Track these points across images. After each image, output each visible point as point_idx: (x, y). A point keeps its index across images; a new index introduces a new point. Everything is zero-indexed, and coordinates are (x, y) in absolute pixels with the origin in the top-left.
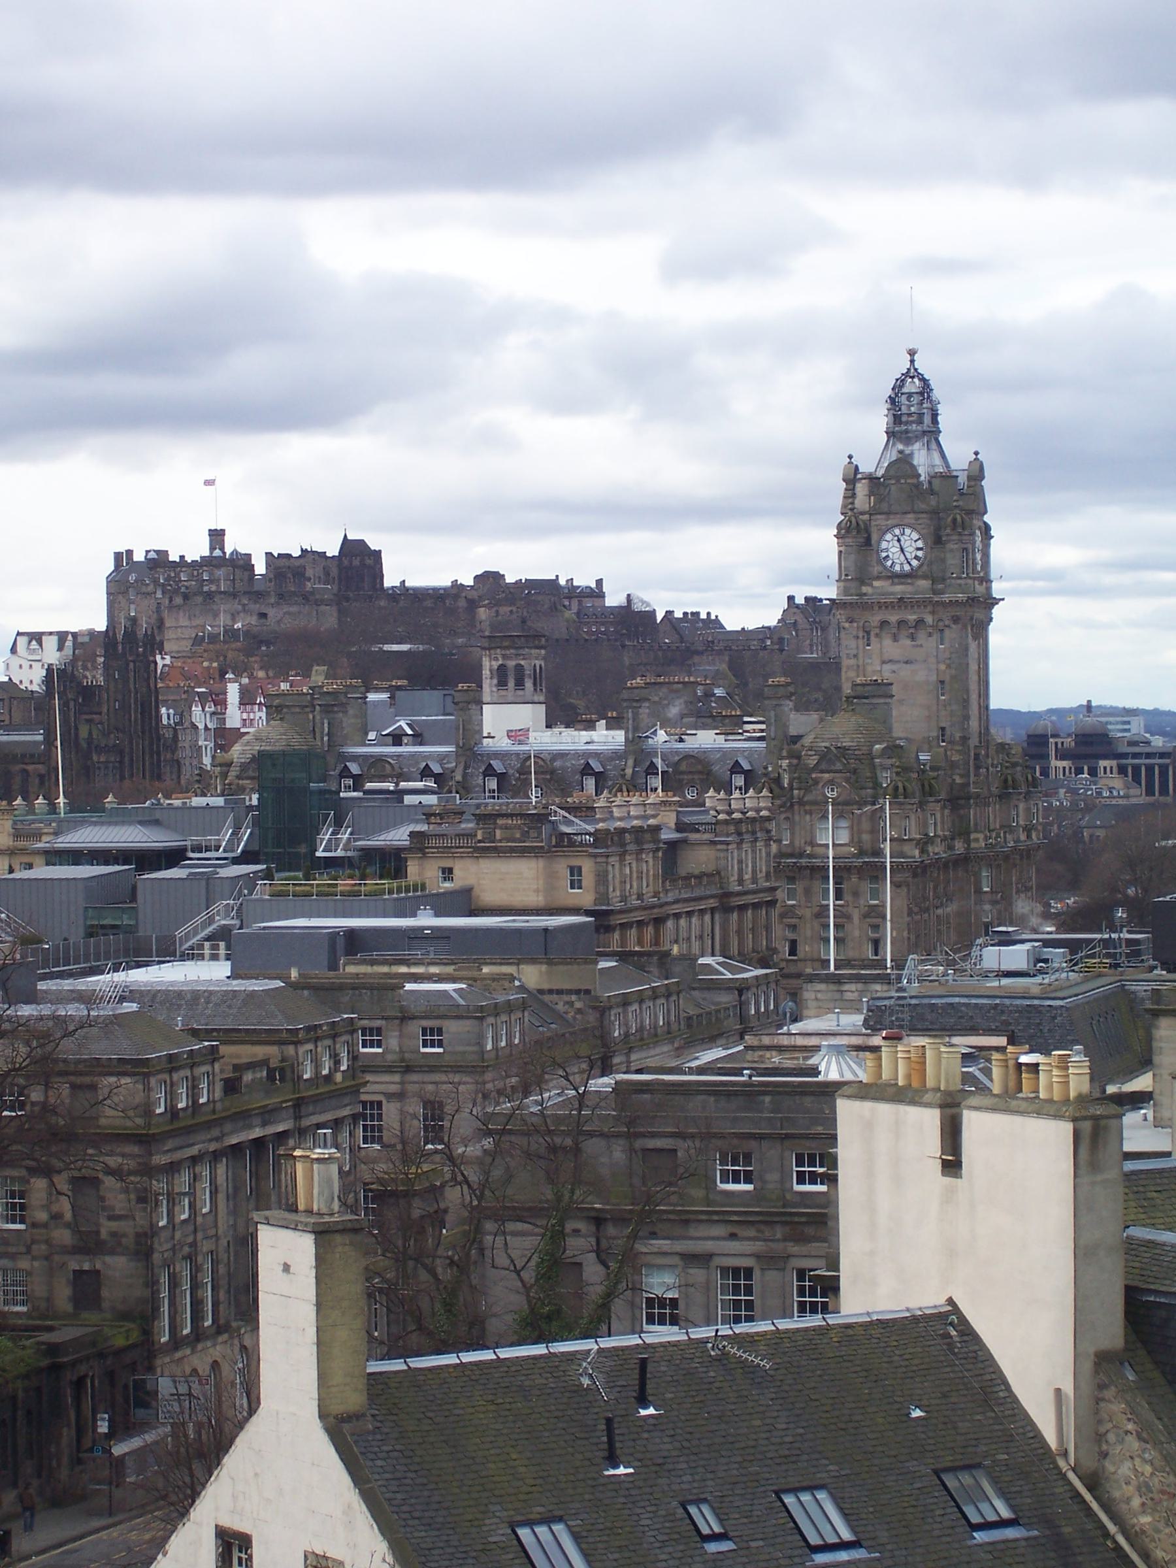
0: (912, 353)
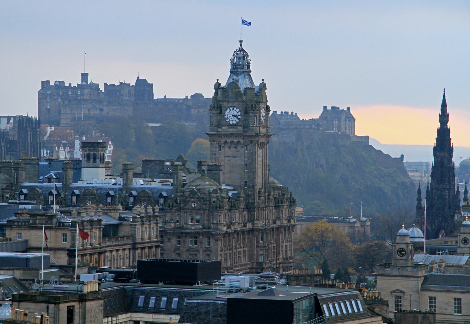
0: (241, 42)
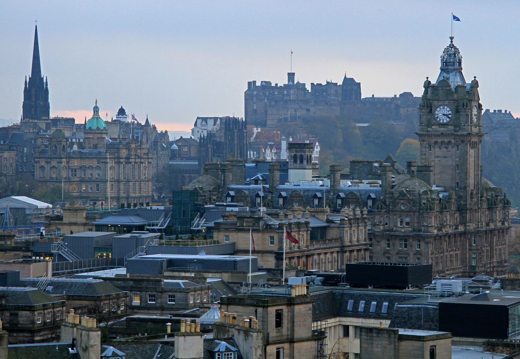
0: (452, 38)
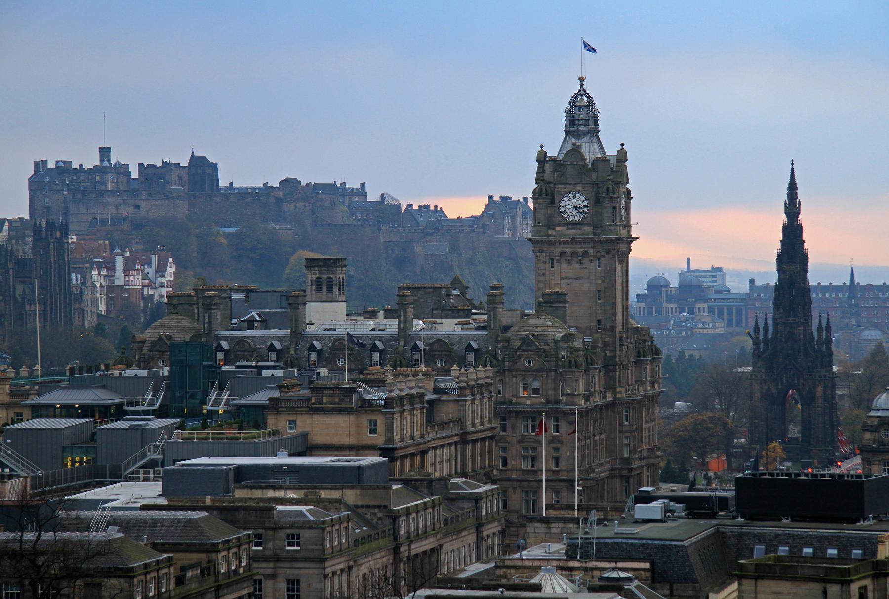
0: (582, 80)
